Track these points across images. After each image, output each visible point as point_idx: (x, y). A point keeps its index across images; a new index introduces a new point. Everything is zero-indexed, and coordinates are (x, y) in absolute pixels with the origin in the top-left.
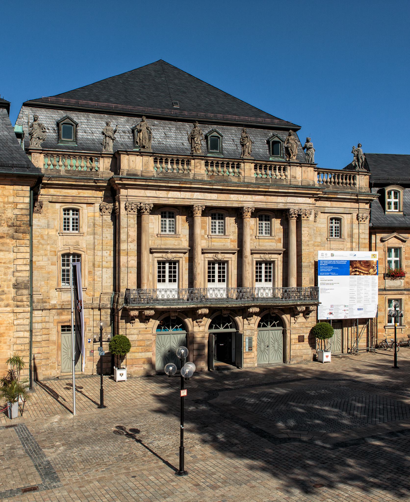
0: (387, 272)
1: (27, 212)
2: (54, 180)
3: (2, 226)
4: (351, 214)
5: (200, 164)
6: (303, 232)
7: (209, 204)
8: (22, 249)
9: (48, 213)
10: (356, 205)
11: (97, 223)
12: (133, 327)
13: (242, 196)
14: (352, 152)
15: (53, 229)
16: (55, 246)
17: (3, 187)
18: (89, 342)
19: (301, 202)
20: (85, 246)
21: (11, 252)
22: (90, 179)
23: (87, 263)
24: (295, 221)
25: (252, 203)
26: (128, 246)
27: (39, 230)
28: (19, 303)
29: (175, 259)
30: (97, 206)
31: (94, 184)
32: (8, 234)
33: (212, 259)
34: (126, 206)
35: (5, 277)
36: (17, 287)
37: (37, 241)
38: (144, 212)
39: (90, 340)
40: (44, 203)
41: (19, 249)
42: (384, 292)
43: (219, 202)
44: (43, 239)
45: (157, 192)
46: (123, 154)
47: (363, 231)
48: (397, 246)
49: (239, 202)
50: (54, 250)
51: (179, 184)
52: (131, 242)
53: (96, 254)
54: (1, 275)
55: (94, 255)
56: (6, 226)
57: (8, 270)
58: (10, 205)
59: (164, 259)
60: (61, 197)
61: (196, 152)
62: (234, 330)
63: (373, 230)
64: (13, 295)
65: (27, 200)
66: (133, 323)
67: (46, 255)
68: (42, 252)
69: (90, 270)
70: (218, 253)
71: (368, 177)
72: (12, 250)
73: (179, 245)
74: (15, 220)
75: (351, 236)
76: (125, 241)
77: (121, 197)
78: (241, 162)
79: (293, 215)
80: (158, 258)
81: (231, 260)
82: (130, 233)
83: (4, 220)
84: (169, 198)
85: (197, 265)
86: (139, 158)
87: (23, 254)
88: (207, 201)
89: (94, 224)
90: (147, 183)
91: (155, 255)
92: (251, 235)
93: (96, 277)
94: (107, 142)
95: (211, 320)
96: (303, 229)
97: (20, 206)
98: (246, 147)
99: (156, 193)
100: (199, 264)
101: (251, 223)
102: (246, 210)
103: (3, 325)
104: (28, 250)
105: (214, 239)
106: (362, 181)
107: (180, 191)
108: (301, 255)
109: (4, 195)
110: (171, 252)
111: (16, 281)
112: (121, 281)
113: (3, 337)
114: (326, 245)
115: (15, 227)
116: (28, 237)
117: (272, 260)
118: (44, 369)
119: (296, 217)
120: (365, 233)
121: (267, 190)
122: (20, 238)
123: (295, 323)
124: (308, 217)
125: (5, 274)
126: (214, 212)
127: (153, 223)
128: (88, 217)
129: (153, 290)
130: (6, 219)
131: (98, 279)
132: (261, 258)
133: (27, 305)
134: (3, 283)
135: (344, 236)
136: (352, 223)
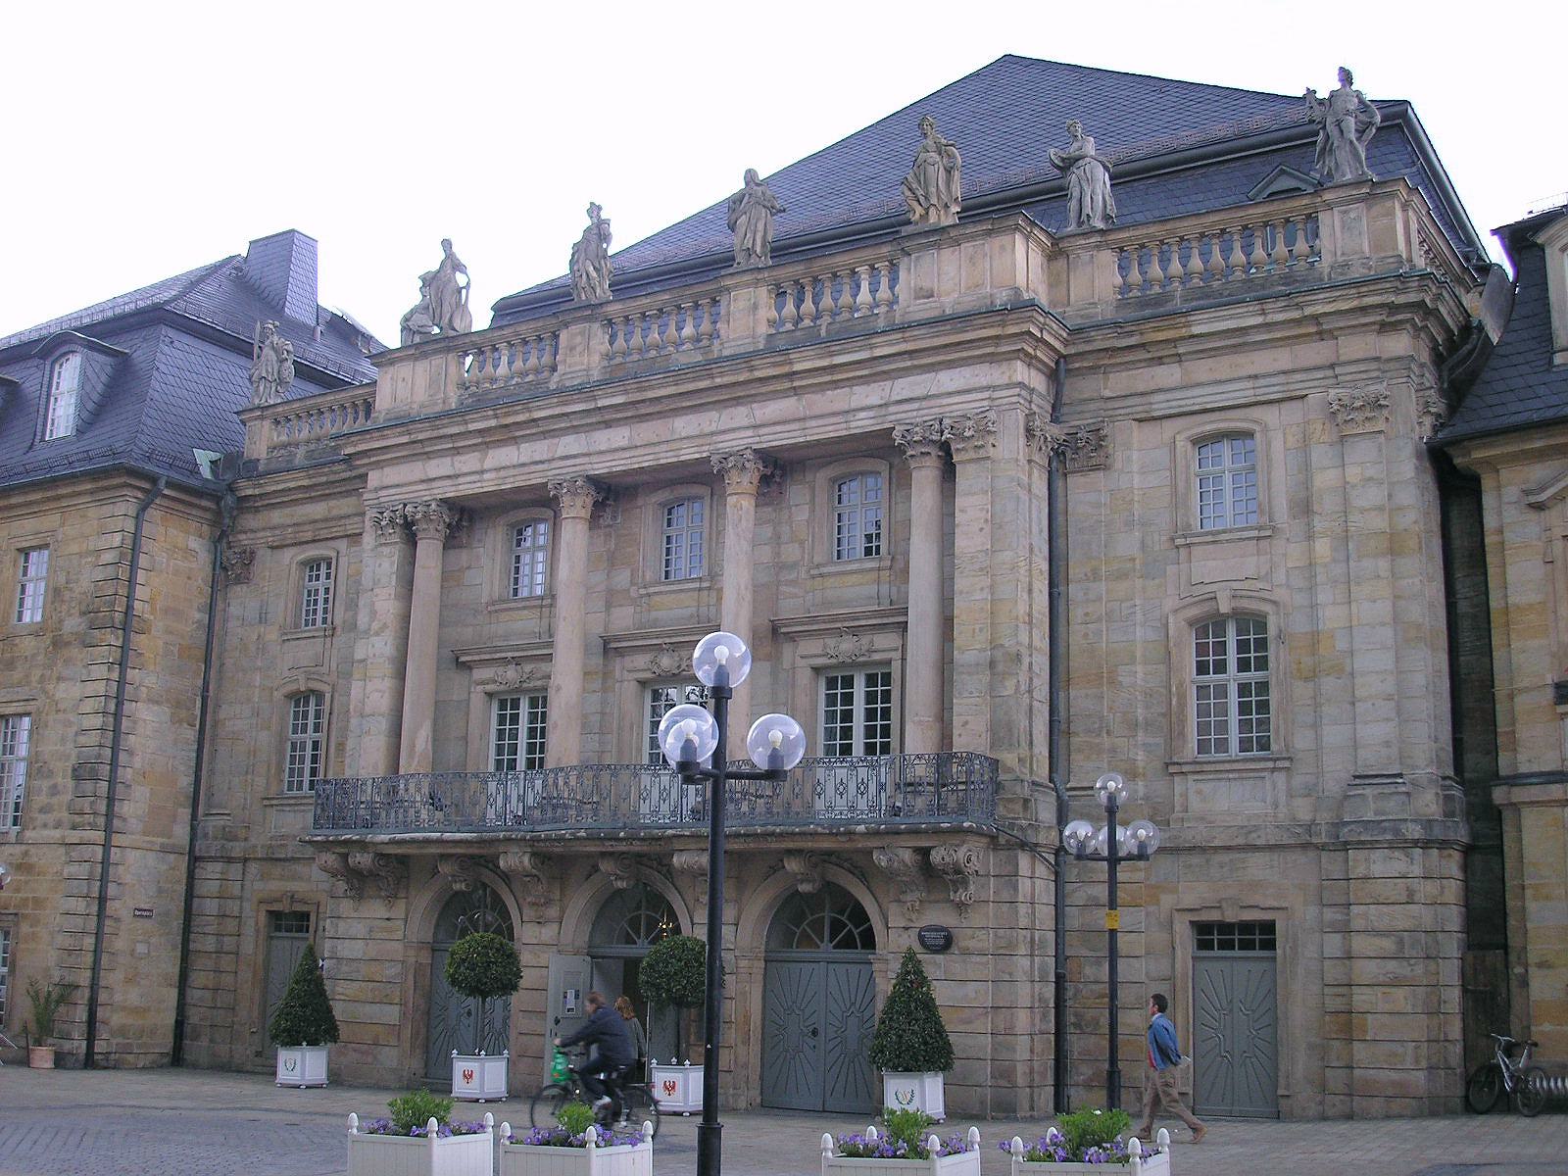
7: (600, 468)
10: (1316, 353)
12: (355, 915)
13: (714, 415)
25: (750, 433)
33: (648, 675)
37: (232, 661)
49: (701, 441)
51: (496, 416)
52: (377, 634)
75: (1304, 508)
85: (554, 692)
100: (559, 689)
105: (657, 598)
114: (1171, 569)
121: (786, 369)
122: (95, 642)
125: (63, 740)
134: (58, 764)
136: (1305, 443)
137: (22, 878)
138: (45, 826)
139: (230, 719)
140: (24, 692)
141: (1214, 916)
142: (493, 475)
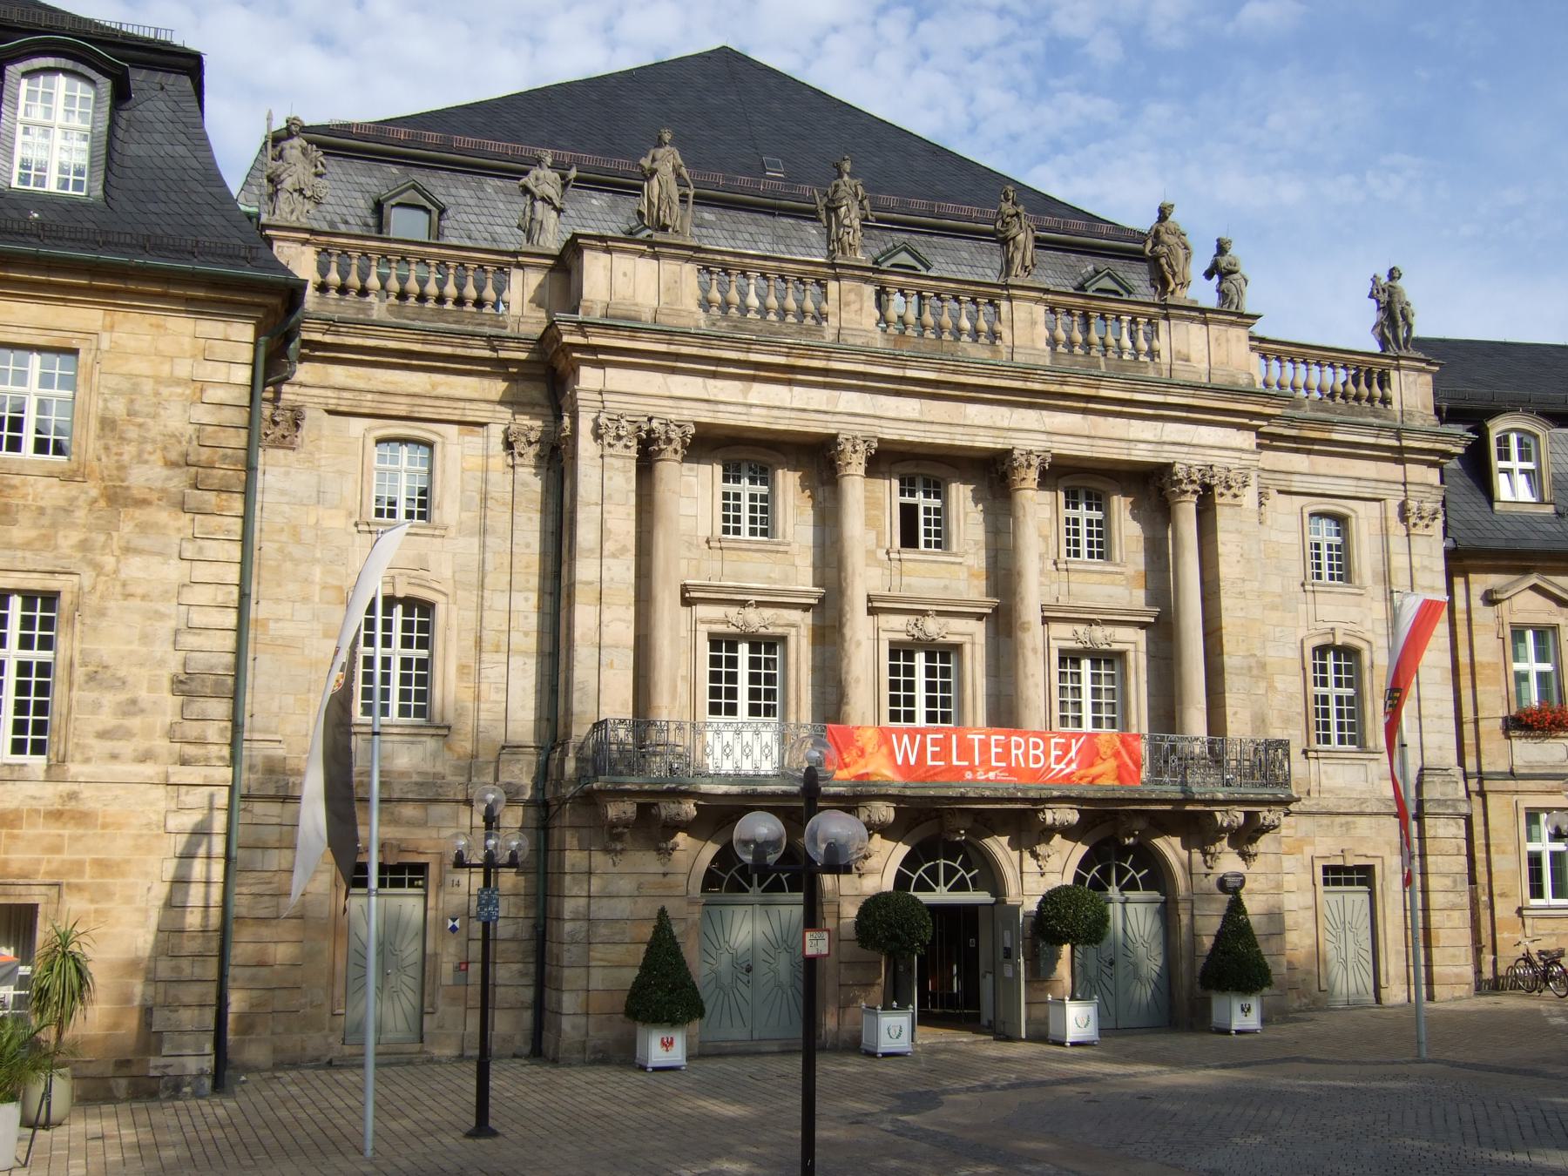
0: (1513, 713)
1: (240, 417)
2: (347, 334)
3: (146, 462)
4: (1379, 500)
5: (860, 295)
6: (1221, 549)
7: (892, 433)
8: (214, 549)
9: (319, 449)
10: (1393, 471)
11: (494, 491)
14: (1371, 296)
15: (336, 507)
16: (342, 570)
17: (158, 326)
18: (454, 929)
19: (1210, 443)
20: (449, 574)
21: (170, 557)
22: (473, 335)
23: (453, 634)
24: (1193, 507)
25: (1044, 437)
26: (604, 565)
27: (286, 508)
28: (190, 750)
29: (771, 630)
30: (496, 432)
31: (487, 353)
32: (163, 490)
33: (903, 637)
34: (597, 426)
35: (144, 650)
36: (185, 687)
38: (661, 450)
39: (457, 923)
40: (308, 413)
41: (201, 549)
42: (1512, 785)
43: (928, 427)
44: (299, 542)
45: (711, 382)
46: (592, 248)
47: (1426, 562)
48: (1542, 619)
49: (996, 433)
50: (335, 583)
51: (788, 355)
52: (614, 556)
53: (486, 604)
54: (130, 642)
55: (481, 607)
56: (161, 463)
57: (158, 624)
58: (179, 390)
59: (733, 629)
60: (369, 396)
61: (844, 253)
62: (983, 897)
63: (1459, 561)
64: (168, 720)
65: (243, 375)
66: (616, 852)
67: (306, 600)
68: (292, 588)
69: (464, 661)
70: (924, 613)
71: (1429, 378)
72: (176, 550)
73: (786, 579)
74: (195, 443)
76: (591, 550)
77: (580, 395)
78: (1000, 296)
79: (1183, 486)
80: (710, 622)
81: (973, 644)
82: (611, 524)
83: (154, 441)
84: (751, 406)
86: (646, 266)
87: (214, 567)
88: (883, 423)
89: (485, 498)
90: (673, 349)
91: (702, 611)
92: (1041, 556)
93: (484, 687)
94: (539, 216)
95: (907, 849)
96: (1221, 536)
97: (214, 395)
98: (1017, 248)
99: (705, 387)
100: (859, 644)
101: (1039, 511)
102: (1023, 459)
103: (125, 831)
104: (235, 552)
106: (1412, 392)
107: (790, 382)
108: (1220, 628)
109: (158, 353)
110: (759, 604)
111: (185, 665)
112: (576, 696)
113: (123, 874)
115: (193, 470)
116: (237, 505)
117: (1116, 647)
118: (280, 1029)
119: (1195, 492)
120: (1431, 570)
121: (1092, 392)
123: (1207, 875)
124: (1235, 496)
126: (909, 469)
127: (694, 492)
128: (463, 470)
129: (694, 726)
130: (159, 438)
131: (494, 697)
132: (1077, 640)
133: (221, 758)
134: (135, 670)
135: (1360, 576)
136: (1385, 533)
137: (66, 832)
138: (114, 757)
139: (278, 620)
140: (46, 560)
141: (1339, 862)
142: (764, 412)
